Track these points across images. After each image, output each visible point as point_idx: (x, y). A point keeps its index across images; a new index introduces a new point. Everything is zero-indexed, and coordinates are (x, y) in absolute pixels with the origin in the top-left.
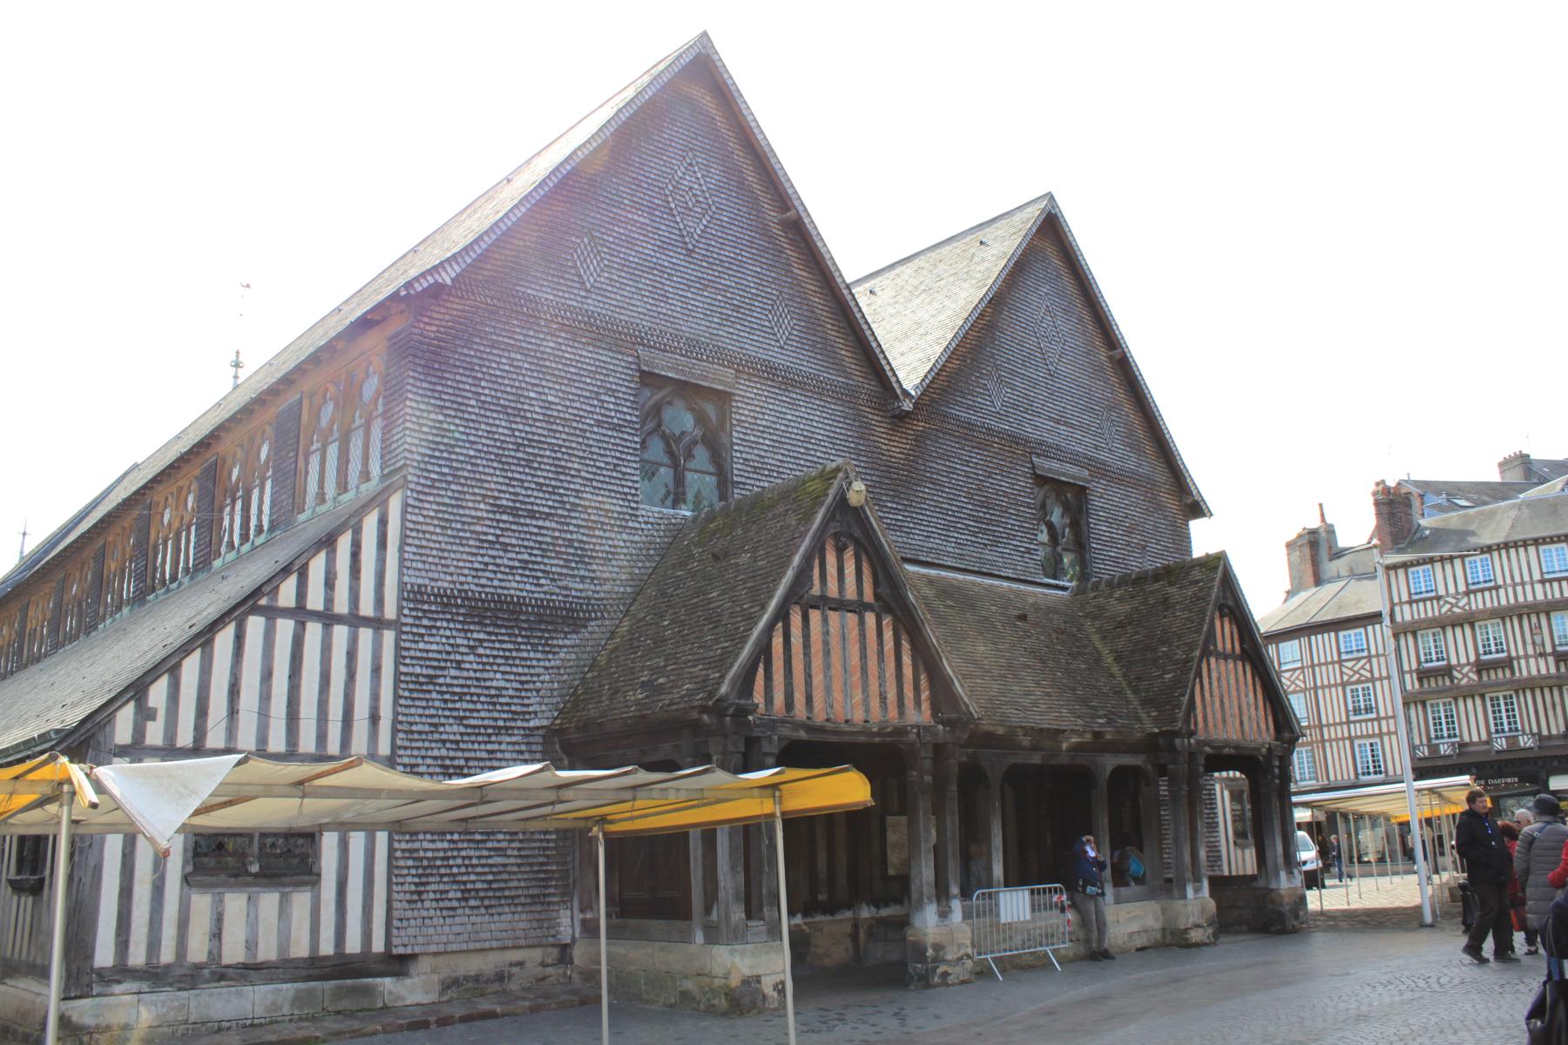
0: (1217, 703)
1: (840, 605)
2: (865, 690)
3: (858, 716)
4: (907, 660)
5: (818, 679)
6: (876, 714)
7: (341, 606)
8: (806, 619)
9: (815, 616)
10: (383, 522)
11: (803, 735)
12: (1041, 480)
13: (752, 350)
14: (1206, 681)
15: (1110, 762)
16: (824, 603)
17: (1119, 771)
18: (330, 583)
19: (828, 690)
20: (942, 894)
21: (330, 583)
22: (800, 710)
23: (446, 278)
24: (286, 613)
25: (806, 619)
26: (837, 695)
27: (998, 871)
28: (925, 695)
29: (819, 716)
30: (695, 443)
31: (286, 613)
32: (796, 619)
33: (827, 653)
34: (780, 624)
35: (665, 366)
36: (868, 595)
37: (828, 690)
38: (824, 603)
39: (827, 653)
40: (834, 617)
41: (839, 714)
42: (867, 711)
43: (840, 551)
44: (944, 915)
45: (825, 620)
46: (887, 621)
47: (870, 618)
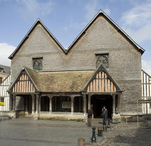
0: (97, 87)
1: (24, 81)
2: (26, 89)
3: (25, 92)
4: (32, 85)
5: (20, 88)
6: (27, 91)
7: (6, 85)
8: (19, 83)
9: (21, 82)
10: (9, 77)
11: (18, 94)
12: (96, 55)
13: (45, 52)
14: (94, 84)
15: (73, 96)
16: (22, 81)
17: (75, 97)
18: (5, 83)
19: (21, 89)
20: (35, 111)
21: (5, 83)
22: (18, 92)
23: (12, 56)
24: (2, 86)
25: (19, 83)
26: (22, 90)
27: (51, 109)
28: (34, 89)
29: (20, 92)
30: (40, 64)
31: (2, 86)
32: (18, 83)
33: (22, 86)
34: (16, 84)
35: (35, 56)
36: (27, 80)
37: (21, 89)
38: (22, 81)
39: (22, 86)
40: (23, 82)
41: (22, 92)
42: (26, 91)
43: (24, 75)
44: (35, 113)
45: (22, 82)
46: (30, 82)
47: (27, 82)
